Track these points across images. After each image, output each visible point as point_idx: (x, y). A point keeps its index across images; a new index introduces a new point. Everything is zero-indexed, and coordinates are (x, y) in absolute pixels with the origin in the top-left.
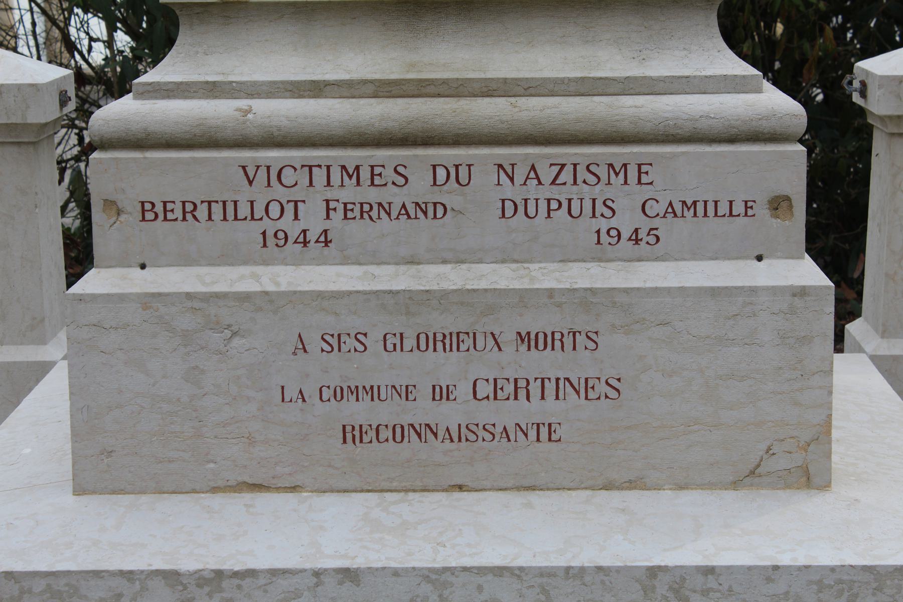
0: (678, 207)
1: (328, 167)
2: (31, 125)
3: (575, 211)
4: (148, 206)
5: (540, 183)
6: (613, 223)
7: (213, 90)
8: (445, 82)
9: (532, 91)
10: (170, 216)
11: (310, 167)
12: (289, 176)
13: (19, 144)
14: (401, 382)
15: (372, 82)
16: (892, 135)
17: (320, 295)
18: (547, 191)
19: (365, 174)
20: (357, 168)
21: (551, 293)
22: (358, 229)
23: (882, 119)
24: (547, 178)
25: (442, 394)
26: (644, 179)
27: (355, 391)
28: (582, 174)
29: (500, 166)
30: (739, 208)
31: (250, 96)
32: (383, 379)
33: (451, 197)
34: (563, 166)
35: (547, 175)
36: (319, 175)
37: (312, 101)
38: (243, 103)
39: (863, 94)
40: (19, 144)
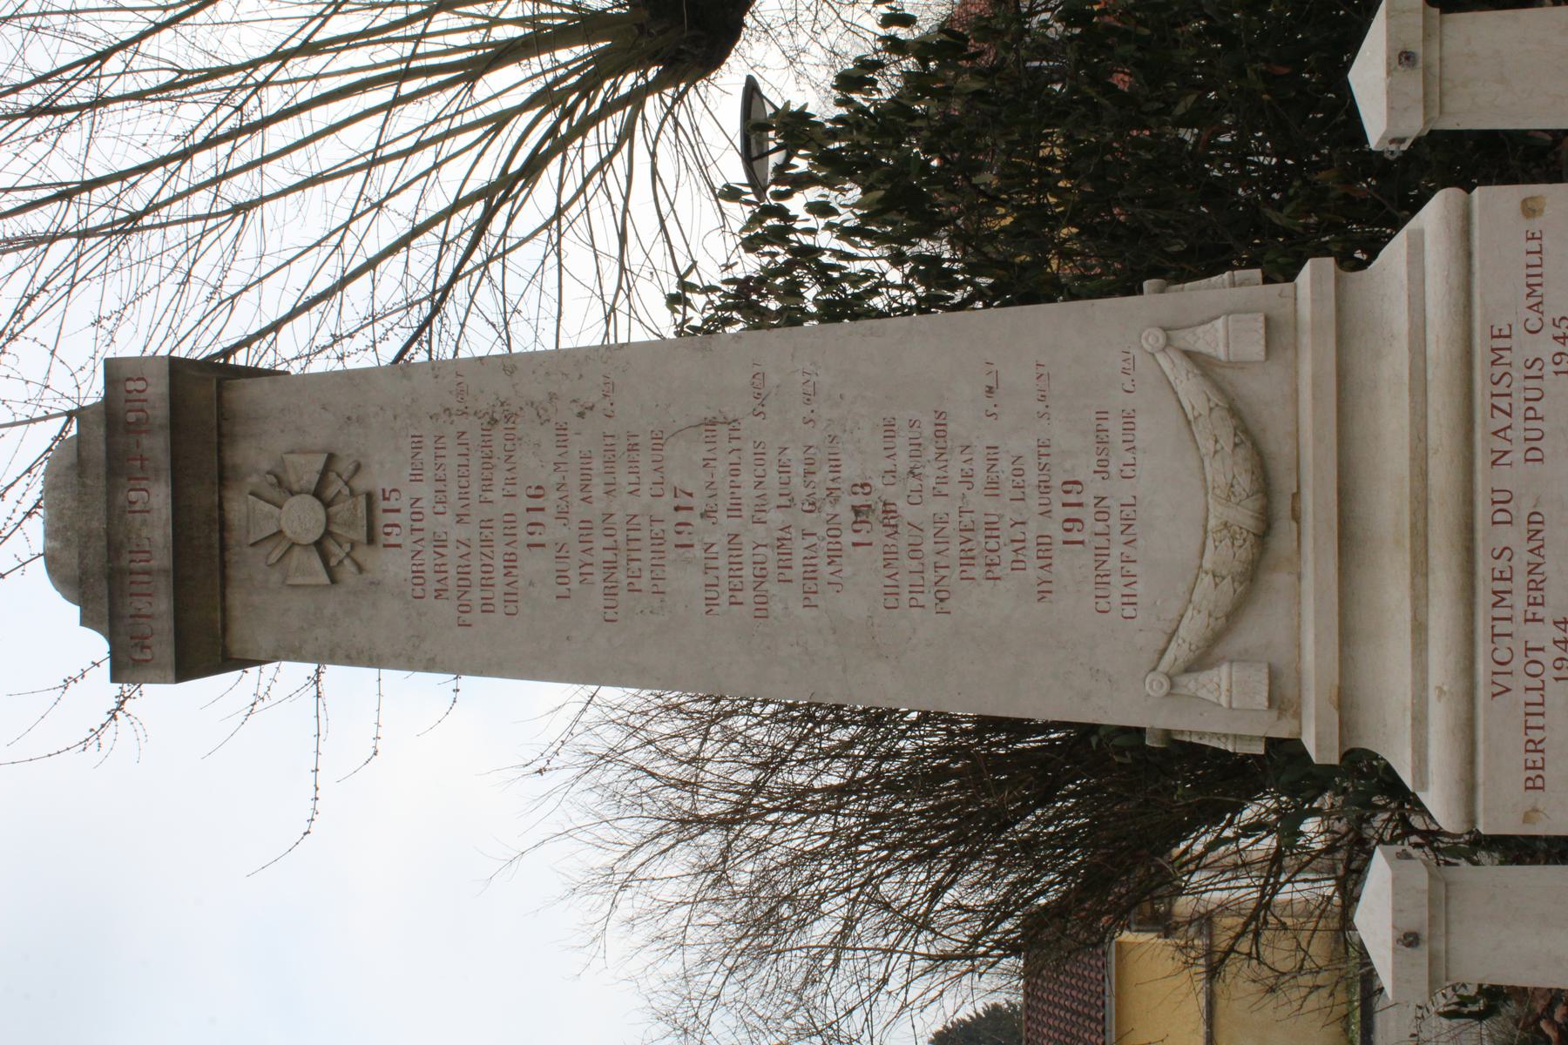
0: (1533, 301)
1: (1494, 619)
2: (1430, 885)
3: (1537, 394)
4: (1530, 784)
5: (1509, 427)
6: (1547, 359)
7: (1420, 720)
8: (1413, 513)
9: (1422, 435)
10: (1539, 764)
11: (1494, 635)
12: (1502, 655)
13: (1447, 898)
15: (1413, 578)
16: (1441, 112)
18: (1518, 420)
19: (1501, 586)
20: (1495, 593)
23: (1426, 123)
24: (1506, 421)
26: (1506, 332)
28: (1501, 389)
29: (1494, 463)
30: (1534, 246)
31: (1425, 687)
33: (1522, 508)
34: (1493, 406)
35: (1503, 421)
36: (1501, 627)
37: (1431, 633)
38: (1432, 694)
40: (1447, 898)
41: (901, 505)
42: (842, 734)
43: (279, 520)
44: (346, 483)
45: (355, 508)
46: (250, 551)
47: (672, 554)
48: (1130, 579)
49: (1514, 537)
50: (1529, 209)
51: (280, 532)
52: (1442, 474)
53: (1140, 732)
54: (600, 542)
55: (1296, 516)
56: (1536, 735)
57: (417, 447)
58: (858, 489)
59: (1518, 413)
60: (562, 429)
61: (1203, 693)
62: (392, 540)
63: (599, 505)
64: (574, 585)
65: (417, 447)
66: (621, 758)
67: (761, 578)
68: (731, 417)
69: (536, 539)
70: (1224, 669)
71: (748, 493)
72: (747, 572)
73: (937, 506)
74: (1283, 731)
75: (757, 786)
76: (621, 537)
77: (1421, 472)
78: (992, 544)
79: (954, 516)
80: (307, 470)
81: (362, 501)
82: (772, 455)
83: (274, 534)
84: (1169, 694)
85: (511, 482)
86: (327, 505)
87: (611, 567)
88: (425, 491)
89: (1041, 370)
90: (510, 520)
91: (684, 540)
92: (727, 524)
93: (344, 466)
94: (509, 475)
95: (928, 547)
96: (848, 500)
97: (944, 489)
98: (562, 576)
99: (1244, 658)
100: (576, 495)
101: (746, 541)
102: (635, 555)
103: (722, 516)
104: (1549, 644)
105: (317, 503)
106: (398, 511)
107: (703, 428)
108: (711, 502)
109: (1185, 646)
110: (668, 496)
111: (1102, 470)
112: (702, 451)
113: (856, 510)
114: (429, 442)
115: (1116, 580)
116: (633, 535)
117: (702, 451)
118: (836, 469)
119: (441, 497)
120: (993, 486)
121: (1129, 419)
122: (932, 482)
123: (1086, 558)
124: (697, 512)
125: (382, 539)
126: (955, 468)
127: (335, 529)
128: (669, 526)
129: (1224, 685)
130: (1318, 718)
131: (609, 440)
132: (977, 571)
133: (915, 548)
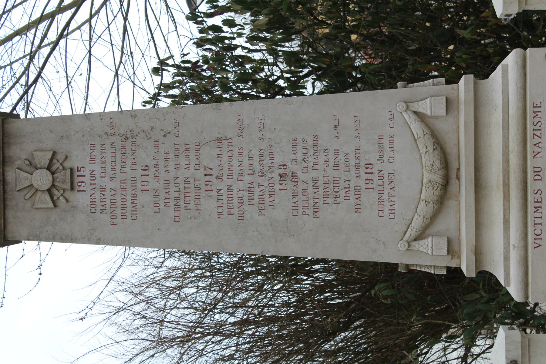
1: (535, 218)
2: (522, 340)
5: (540, 142)
7: (507, 258)
8: (504, 176)
9: (507, 146)
11: (535, 224)
12: (538, 232)
13: (529, 346)
15: (504, 202)
16: (526, 4)
19: (537, 205)
20: (535, 207)
23: (519, 8)
24: (539, 140)
26: (539, 105)
28: (537, 127)
29: (534, 157)
31: (509, 245)
34: (534, 134)
35: (537, 140)
36: (538, 221)
37: (511, 223)
38: (511, 248)
39: (510, 15)
40: (529, 346)
41: (299, 173)
42: (244, 295)
43: (31, 180)
44: (61, 164)
45: (65, 175)
46: (17, 193)
47: (204, 194)
48: (392, 202)
51: (32, 185)
53: (395, 266)
54: (173, 189)
55: (458, 178)
57: (93, 149)
58: (281, 167)
60: (157, 141)
61: (421, 249)
62: (81, 188)
63: (172, 174)
64: (162, 207)
65: (93, 149)
66: (129, 308)
67: (241, 204)
68: (228, 137)
69: (145, 188)
70: (430, 239)
71: (236, 169)
72: (235, 201)
73: (314, 174)
74: (453, 264)
75: (199, 323)
76: (182, 187)
78: (336, 189)
79: (321, 178)
80: (44, 158)
81: (69, 172)
82: (246, 152)
83: (28, 186)
84: (407, 250)
85: (134, 164)
86: (53, 173)
87: (177, 199)
88: (97, 168)
89: (356, 119)
91: (208, 188)
93: (60, 157)
94: (133, 161)
95: (310, 190)
96: (277, 172)
97: (317, 167)
98: (156, 203)
99: (438, 235)
100: (162, 169)
101: (235, 188)
102: (187, 194)
103: (224, 178)
105: (49, 172)
106: (84, 176)
107: (217, 141)
108: (220, 172)
109: (414, 230)
110: (202, 169)
111: (381, 159)
112: (216, 151)
113: (281, 176)
114: (98, 147)
115: (387, 204)
116: (187, 186)
117: (216, 151)
118: (272, 158)
119: (103, 170)
120: (337, 166)
121: (392, 139)
122: (312, 164)
123: (374, 195)
124: (214, 176)
125: (77, 188)
126: (321, 158)
127: (56, 184)
128: (202, 182)
129: (430, 245)
130: (467, 258)
131: (177, 147)
132: (330, 200)
133: (305, 191)
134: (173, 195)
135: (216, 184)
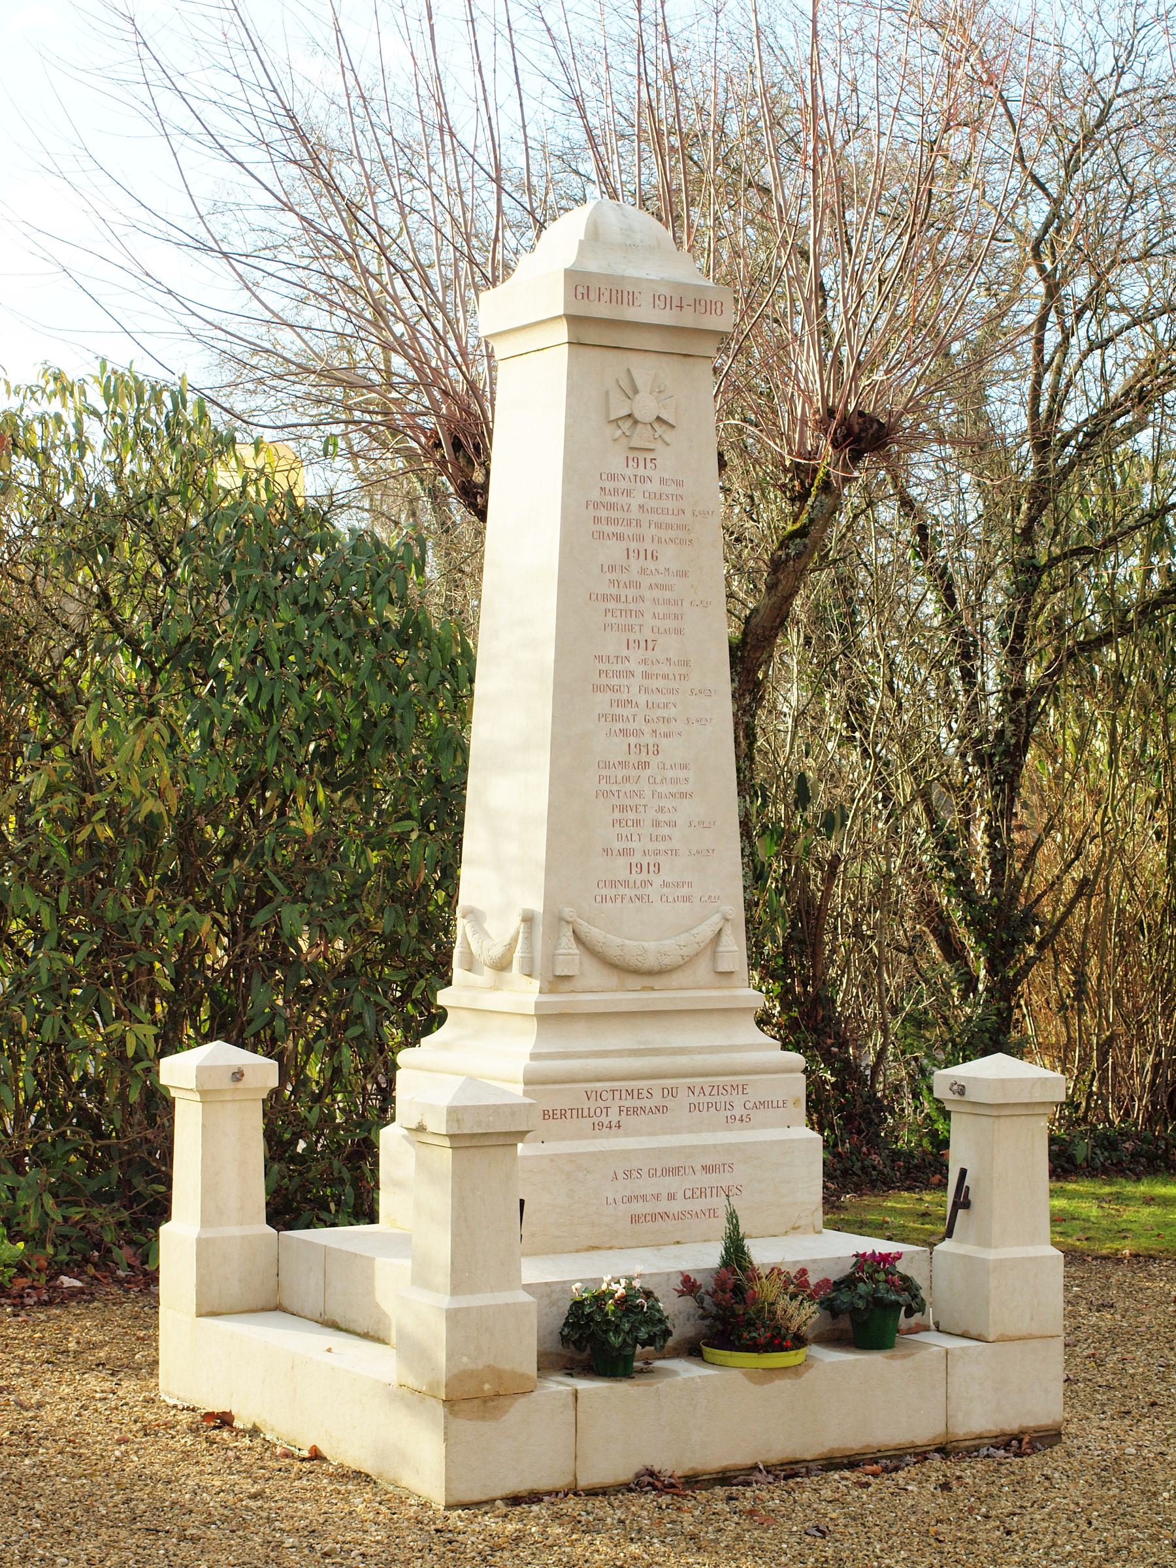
6: (733, 1113)
14: (655, 1192)
17: (624, 1151)
18: (708, 1099)
21: (715, 1146)
22: (633, 1119)
24: (707, 1093)
25: (671, 1197)
27: (636, 1197)
32: (648, 1191)
36: (617, 1094)
41: (648, 772)
48: (614, 899)
49: (657, 1100)
50: (796, 1102)
52: (683, 1062)
54: (631, 593)
55: (644, 989)
56: (568, 1114)
59: (710, 1099)
63: (649, 595)
64: (609, 576)
67: (612, 689)
72: (615, 681)
73: (648, 793)
76: (632, 606)
77: (701, 1050)
78: (630, 823)
79: (643, 802)
82: (672, 698)
85: (660, 541)
88: (654, 487)
90: (641, 538)
92: (639, 669)
93: (669, 436)
95: (628, 787)
103: (643, 668)
104: (609, 1119)
111: (665, 884)
112: (674, 659)
118: (666, 735)
120: (656, 824)
121: (687, 899)
122: (659, 790)
123: (623, 874)
126: (668, 803)
133: (628, 779)
134: (623, 592)
135: (636, 655)
